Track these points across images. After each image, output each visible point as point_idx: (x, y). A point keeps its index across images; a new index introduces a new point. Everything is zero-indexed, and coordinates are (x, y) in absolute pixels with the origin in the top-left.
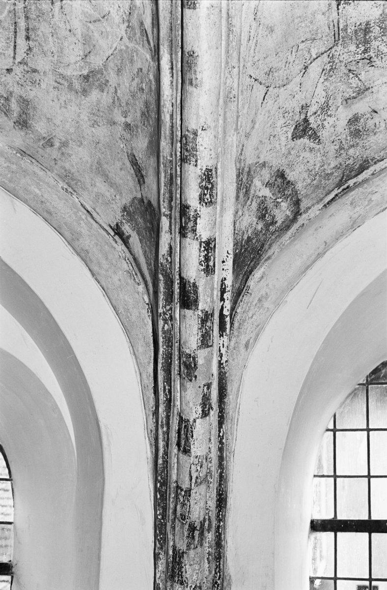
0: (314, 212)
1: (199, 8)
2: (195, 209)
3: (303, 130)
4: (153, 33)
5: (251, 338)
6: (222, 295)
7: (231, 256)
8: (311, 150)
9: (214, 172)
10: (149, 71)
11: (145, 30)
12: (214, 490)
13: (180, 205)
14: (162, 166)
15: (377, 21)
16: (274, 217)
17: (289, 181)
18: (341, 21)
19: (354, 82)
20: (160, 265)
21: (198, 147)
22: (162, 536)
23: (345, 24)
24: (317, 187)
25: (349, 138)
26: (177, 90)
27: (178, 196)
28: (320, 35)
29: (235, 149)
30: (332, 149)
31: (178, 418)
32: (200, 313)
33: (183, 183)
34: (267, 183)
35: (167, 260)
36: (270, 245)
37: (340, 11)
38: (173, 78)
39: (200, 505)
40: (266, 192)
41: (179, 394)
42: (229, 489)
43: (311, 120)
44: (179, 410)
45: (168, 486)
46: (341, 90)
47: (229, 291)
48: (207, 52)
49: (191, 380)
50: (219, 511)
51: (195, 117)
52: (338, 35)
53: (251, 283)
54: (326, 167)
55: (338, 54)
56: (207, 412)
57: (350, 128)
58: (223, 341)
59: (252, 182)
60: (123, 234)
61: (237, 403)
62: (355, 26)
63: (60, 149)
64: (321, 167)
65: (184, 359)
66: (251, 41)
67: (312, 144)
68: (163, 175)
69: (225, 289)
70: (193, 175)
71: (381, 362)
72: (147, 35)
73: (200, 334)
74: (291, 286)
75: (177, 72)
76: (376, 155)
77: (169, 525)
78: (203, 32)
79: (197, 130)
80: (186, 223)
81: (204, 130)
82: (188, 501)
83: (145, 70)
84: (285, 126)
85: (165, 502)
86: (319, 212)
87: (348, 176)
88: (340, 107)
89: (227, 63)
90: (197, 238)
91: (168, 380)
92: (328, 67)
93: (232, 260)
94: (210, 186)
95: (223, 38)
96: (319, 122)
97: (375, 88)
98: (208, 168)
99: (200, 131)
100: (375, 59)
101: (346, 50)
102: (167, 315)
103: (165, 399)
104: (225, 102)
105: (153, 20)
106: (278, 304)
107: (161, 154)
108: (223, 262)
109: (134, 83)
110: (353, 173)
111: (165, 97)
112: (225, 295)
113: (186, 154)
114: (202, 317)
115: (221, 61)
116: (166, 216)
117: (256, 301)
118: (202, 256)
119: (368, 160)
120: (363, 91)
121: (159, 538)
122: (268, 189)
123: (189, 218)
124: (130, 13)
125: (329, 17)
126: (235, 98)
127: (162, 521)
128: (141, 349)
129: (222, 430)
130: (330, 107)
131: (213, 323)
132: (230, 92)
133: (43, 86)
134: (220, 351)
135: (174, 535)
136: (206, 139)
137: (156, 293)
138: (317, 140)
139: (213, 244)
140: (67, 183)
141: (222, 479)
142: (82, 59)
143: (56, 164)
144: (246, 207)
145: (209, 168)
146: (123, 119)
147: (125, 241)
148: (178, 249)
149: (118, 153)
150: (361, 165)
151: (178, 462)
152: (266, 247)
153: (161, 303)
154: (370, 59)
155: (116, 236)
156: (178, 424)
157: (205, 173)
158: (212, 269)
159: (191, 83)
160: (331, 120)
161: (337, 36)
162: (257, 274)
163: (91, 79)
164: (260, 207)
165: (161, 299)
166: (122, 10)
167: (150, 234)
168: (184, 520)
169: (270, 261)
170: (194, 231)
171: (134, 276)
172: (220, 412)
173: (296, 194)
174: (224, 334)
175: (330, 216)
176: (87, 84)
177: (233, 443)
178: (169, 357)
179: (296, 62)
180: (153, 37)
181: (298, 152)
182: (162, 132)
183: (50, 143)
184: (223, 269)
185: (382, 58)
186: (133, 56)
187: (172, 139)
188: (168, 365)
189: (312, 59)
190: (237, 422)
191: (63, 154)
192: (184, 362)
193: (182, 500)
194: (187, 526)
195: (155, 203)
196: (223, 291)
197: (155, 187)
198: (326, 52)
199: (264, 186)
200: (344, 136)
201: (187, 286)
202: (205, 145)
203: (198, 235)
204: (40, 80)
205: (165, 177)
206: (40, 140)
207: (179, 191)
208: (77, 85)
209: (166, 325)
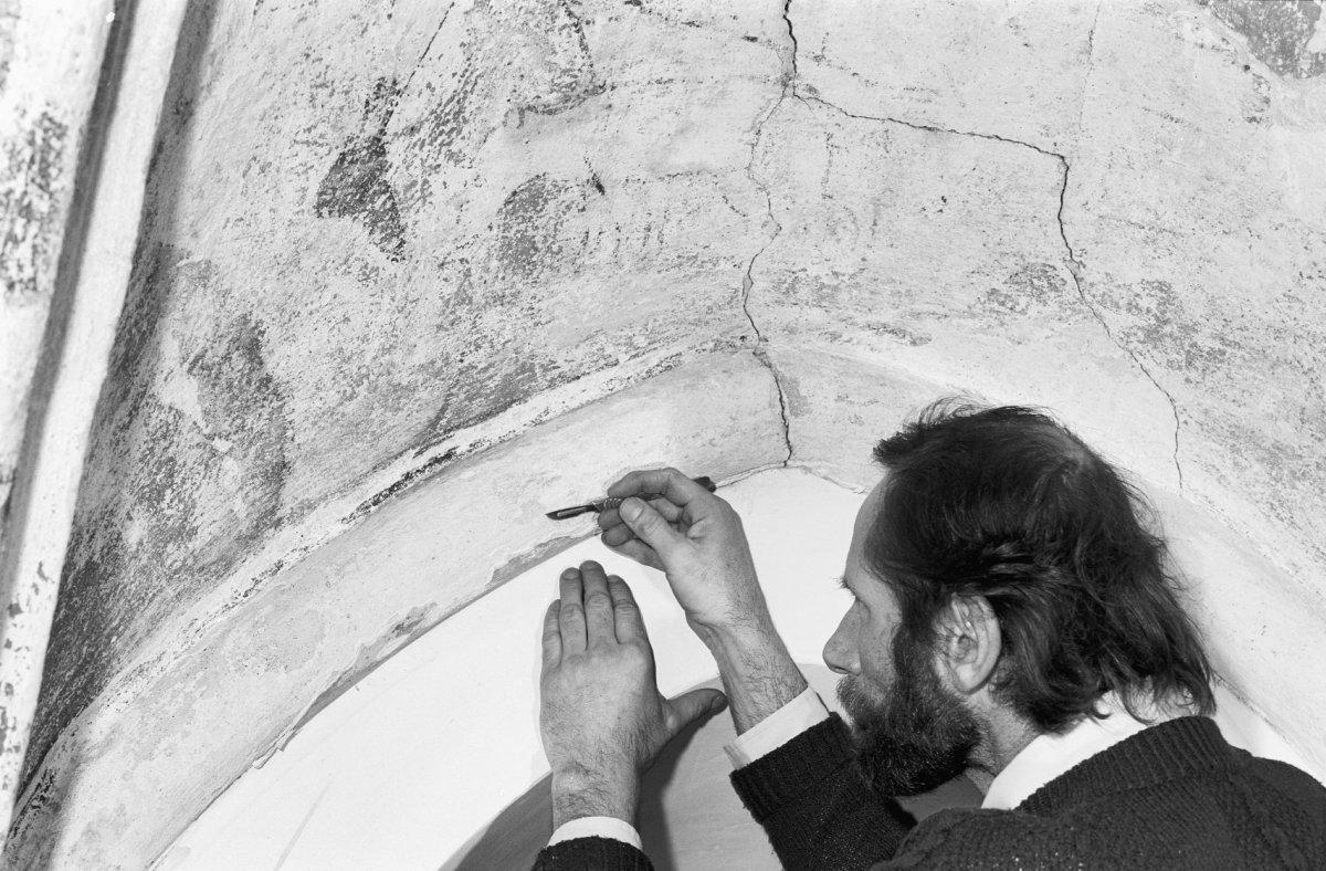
0: (326, 524)
8: (367, 274)
19: (565, 46)
24: (354, 428)
25: (494, 264)
30: (434, 289)
34: (196, 361)
36: (155, 621)
43: (396, 152)
46: (517, 63)
47: (17, 749)
54: (397, 357)
57: (507, 228)
67: (375, 250)
76: (563, 353)
84: (307, 143)
86: (342, 527)
87: (458, 412)
88: (498, 133)
97: (621, 90)
110: (478, 406)
119: (531, 369)
120: (581, 93)
130: (465, 121)
138: (395, 242)
145: (57, 116)
150: (507, 380)
157: (33, 133)
160: (454, 175)
173: (281, 437)
181: (324, 268)
199: (186, 366)
200: (482, 253)
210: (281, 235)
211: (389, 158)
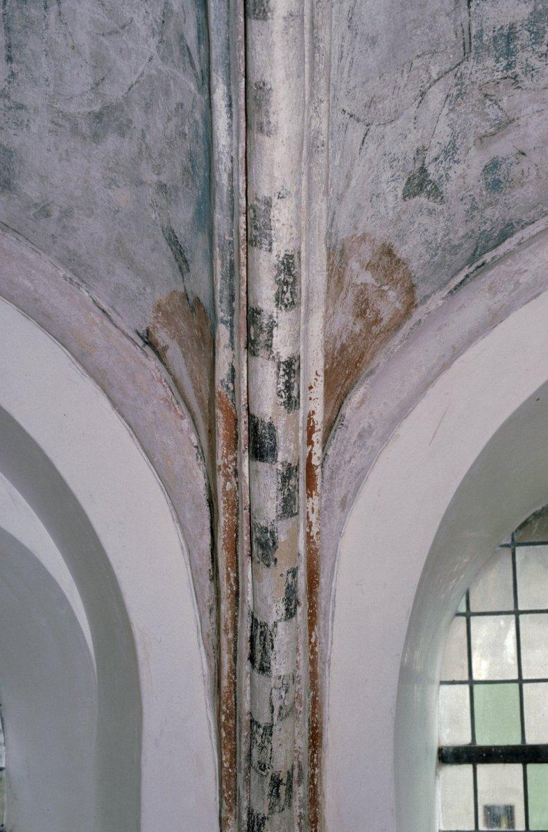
0: (435, 302)
1: (273, 18)
2: (270, 314)
3: (419, 183)
4: (199, 52)
5: (349, 492)
6: (310, 436)
7: (321, 379)
8: (431, 212)
9: (296, 259)
10: (193, 107)
11: (187, 46)
12: (304, 723)
13: (247, 308)
14: (218, 249)
15: (526, 23)
16: (378, 312)
17: (399, 260)
18: (474, 24)
19: (492, 112)
20: (217, 395)
21: (272, 223)
22: (230, 793)
23: (479, 28)
24: (440, 265)
26: (238, 138)
27: (243, 294)
28: (443, 46)
29: (324, 222)
31: (250, 619)
32: (280, 467)
33: (250, 275)
35: (228, 388)
37: (472, 9)
38: (232, 120)
39: (285, 749)
40: (367, 277)
41: (250, 585)
42: (325, 717)
43: (431, 169)
44: (252, 608)
45: (238, 718)
47: (320, 430)
48: (284, 83)
49: (268, 566)
50: (314, 752)
51: (267, 179)
52: (469, 46)
53: (347, 411)
54: (451, 236)
55: (469, 72)
56: (293, 611)
57: (486, 179)
58: (313, 504)
59: (347, 264)
60: (157, 344)
61: (332, 588)
62: (494, 31)
63: (59, 220)
64: (445, 236)
65: (258, 535)
66: (343, 61)
67: (431, 204)
68: (219, 262)
69: (313, 427)
70: (266, 264)
71: (531, 513)
72: (190, 54)
73: (281, 497)
74: (405, 410)
75: (238, 111)
76: (524, 216)
77: (241, 776)
78: (278, 53)
79: (270, 198)
80: (257, 336)
81: (282, 197)
82: (269, 742)
83: (188, 106)
84: (393, 180)
85: (234, 743)
86: (442, 302)
87: (483, 248)
88: (472, 149)
89: (312, 95)
90: (273, 357)
91: (235, 564)
92: (455, 92)
93: (322, 384)
94: (291, 280)
95: (306, 60)
96: (442, 172)
97: (523, 119)
98: (287, 253)
99: (275, 200)
100: (522, 77)
101: (480, 66)
102: (230, 468)
103: (229, 592)
104: (310, 154)
105: (199, 32)
106: (385, 439)
107: (216, 232)
108: (311, 388)
109: (172, 125)
110: (491, 244)
111: (221, 147)
112: (314, 436)
113: (254, 233)
114: (283, 473)
115: (304, 94)
116: (225, 322)
117: (354, 438)
118: (281, 383)
121: (226, 795)
122: (369, 272)
123: (261, 329)
124: (163, 22)
125: (455, 20)
126: (323, 146)
127: (230, 770)
128: (188, 516)
129: (313, 634)
131: (298, 480)
132: (317, 138)
133: (34, 129)
134: (308, 518)
135: (249, 791)
136: (285, 211)
137: (211, 433)
138: (440, 198)
139: (297, 365)
140: (71, 270)
141: (316, 704)
142: (92, 88)
143: (54, 242)
144: (339, 302)
146: (155, 178)
147: (160, 354)
148: (245, 372)
149: (148, 226)
151: (252, 685)
152: (368, 356)
153: (221, 450)
154: (515, 79)
155: (147, 346)
156: (249, 628)
158: (296, 402)
159: (261, 130)
160: (459, 168)
161: (467, 46)
162: (356, 397)
163: (105, 119)
164: (358, 300)
165: (220, 445)
166: (151, 17)
167: (200, 346)
168: (264, 771)
169: (373, 377)
170: (269, 346)
171: (174, 405)
172: (311, 607)
174: (314, 493)
175: (460, 308)
176: (99, 125)
177: (327, 649)
178: (235, 530)
179: (409, 87)
180: (200, 58)
181: (412, 216)
182: (217, 200)
183: (45, 212)
184: (310, 399)
185: (532, 76)
186: (170, 85)
187: (232, 210)
188: (231, 545)
189: (432, 80)
190: (333, 616)
191: (64, 227)
192: (257, 539)
193: (259, 741)
194: (268, 780)
195: (206, 302)
196: (310, 431)
197: (205, 277)
198: (451, 70)
199: (364, 268)
200: (478, 191)
201: (260, 427)
202: (282, 217)
203: (275, 352)
204: (28, 121)
205: (223, 265)
206: (29, 207)
207: (244, 287)
208: (84, 128)
209: (228, 483)
210: (391, 213)
211: (429, 172)
